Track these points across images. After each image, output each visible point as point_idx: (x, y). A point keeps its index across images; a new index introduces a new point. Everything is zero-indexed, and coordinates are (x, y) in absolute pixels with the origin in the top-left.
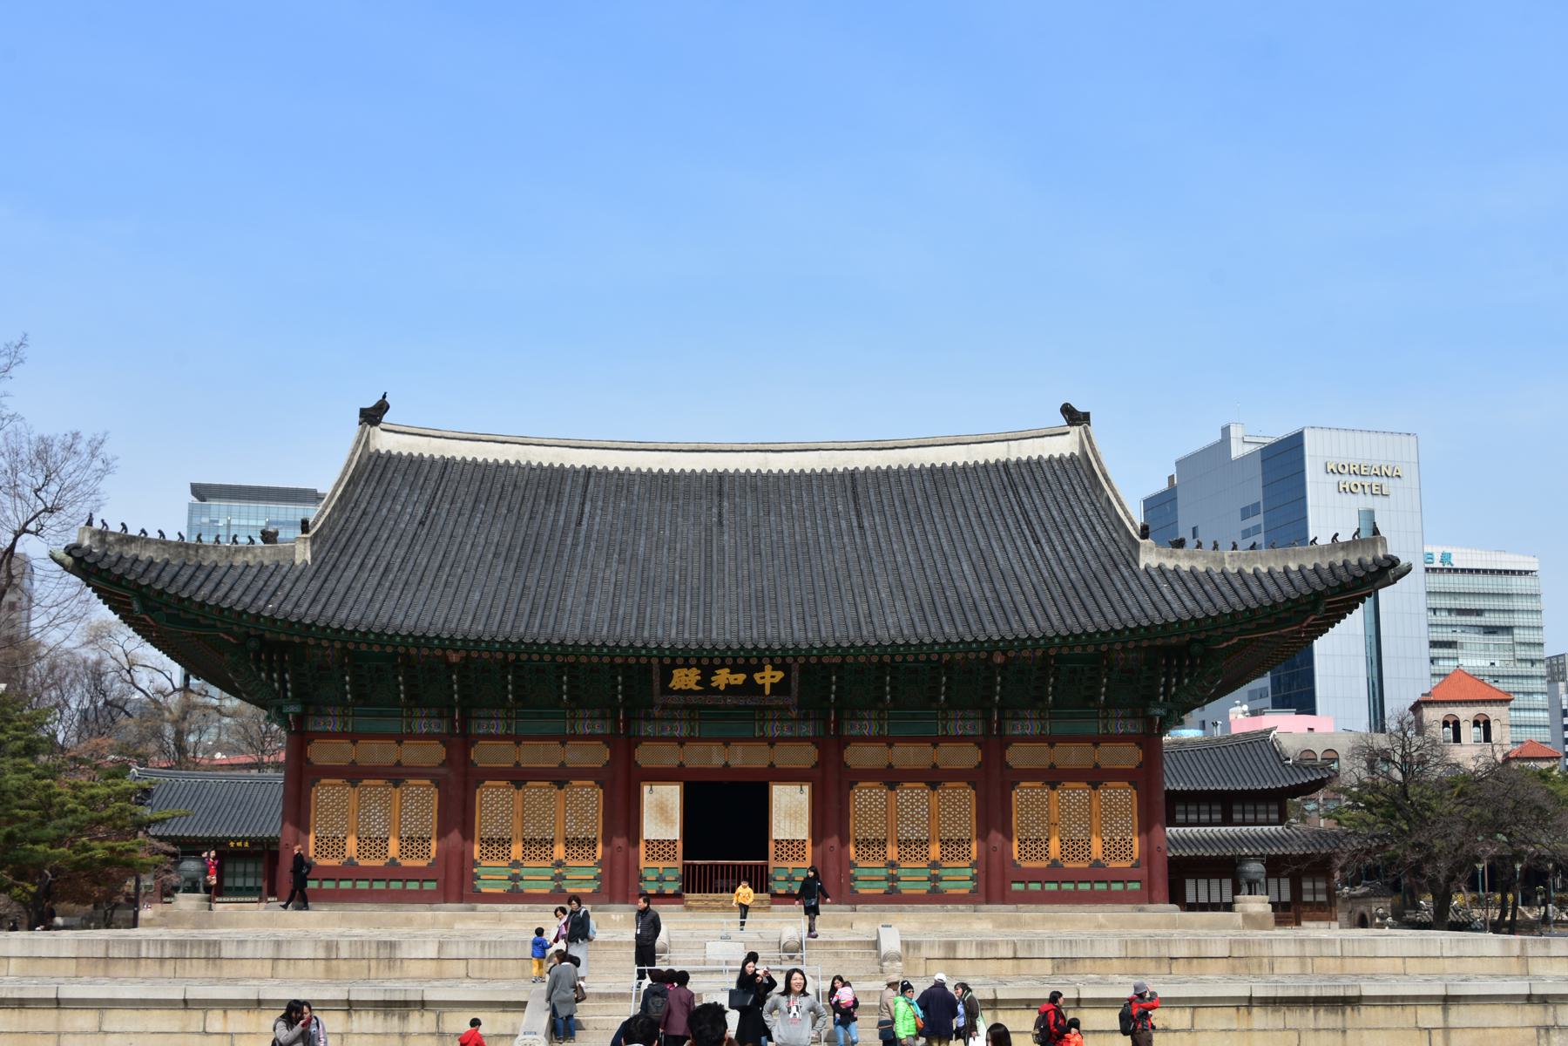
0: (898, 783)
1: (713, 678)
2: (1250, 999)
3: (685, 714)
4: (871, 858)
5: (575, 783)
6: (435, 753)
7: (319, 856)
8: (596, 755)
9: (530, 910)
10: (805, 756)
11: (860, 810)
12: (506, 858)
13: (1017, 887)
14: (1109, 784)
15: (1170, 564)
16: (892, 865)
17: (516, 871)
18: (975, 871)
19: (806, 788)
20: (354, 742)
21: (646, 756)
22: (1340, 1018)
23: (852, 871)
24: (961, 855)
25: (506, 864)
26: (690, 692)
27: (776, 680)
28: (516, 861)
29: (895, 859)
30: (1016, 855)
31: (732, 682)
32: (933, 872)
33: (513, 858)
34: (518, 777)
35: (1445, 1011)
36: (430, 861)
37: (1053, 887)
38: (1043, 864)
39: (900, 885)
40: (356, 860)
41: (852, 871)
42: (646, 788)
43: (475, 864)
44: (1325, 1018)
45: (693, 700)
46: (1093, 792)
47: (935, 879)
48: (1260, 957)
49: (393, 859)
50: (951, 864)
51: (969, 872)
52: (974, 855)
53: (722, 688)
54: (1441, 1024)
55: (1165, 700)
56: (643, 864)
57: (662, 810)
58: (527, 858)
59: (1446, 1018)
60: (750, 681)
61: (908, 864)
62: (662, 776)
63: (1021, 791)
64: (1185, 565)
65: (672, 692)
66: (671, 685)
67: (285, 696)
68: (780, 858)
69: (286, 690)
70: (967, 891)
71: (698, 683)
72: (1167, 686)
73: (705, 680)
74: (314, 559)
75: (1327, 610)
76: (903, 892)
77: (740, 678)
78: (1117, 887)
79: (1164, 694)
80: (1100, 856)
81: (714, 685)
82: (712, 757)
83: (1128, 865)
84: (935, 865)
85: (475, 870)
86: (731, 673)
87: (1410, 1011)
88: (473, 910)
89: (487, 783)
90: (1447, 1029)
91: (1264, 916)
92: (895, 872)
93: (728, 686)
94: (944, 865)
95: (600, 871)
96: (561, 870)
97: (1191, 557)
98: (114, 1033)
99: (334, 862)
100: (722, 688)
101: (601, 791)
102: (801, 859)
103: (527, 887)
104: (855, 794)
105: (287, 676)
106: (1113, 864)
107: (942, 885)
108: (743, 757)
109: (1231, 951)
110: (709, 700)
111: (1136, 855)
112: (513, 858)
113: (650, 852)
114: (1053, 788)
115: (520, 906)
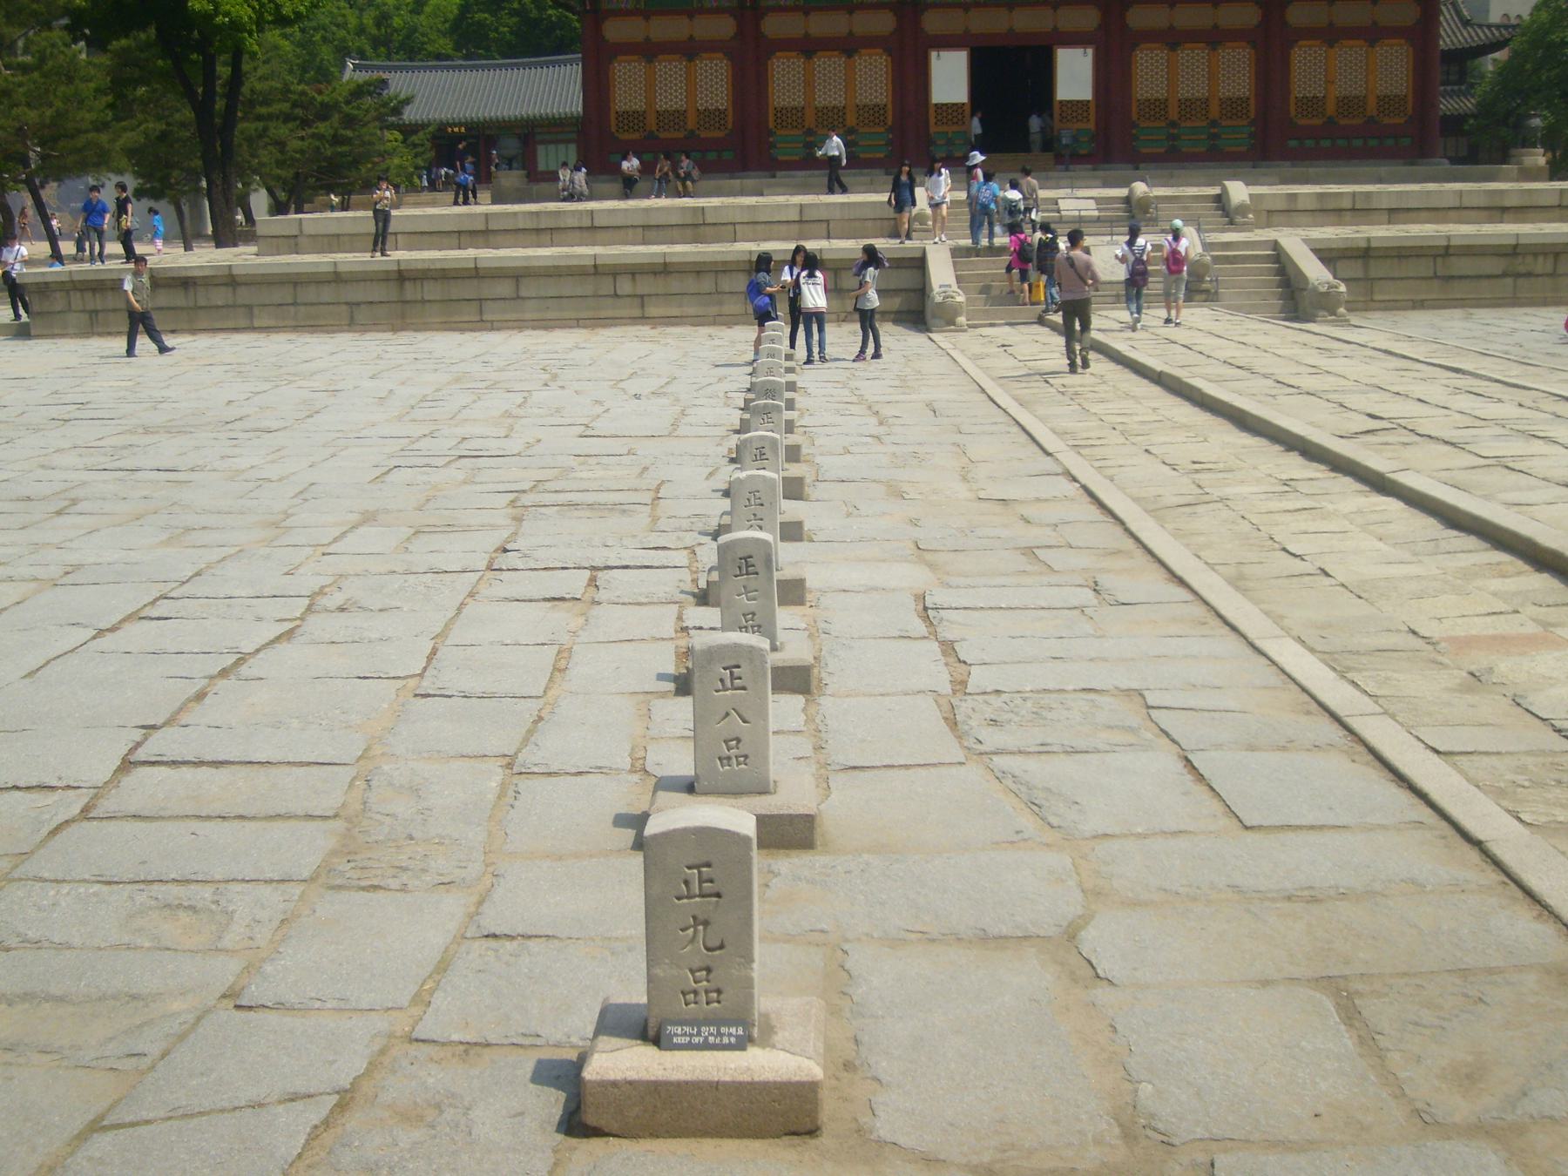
4: (1152, 118)
5: (863, 51)
6: (724, 27)
7: (621, 130)
8: (882, 23)
10: (1087, 18)
11: (1162, 70)
12: (799, 126)
13: (1293, 143)
14: (1386, 41)
16: (1173, 124)
18: (1253, 129)
19: (1090, 51)
20: (647, 18)
21: (933, 22)
23: (1134, 131)
24: (1240, 114)
25: (800, 132)
28: (809, 129)
29: (1176, 118)
30: (1293, 113)
32: (1212, 130)
33: (806, 127)
34: (808, 47)
36: (727, 132)
37: (1326, 143)
38: (1317, 122)
40: (656, 133)
41: (1134, 131)
42: (934, 54)
43: (770, 133)
46: (1370, 49)
47: (1215, 137)
49: (692, 132)
50: (1229, 122)
52: (1252, 115)
56: (933, 129)
58: (779, 127)
61: (1188, 124)
62: (948, 42)
63: (1300, 50)
68: (1065, 120)
70: (1244, 149)
76: (1184, 150)
78: (1390, 142)
80: (1375, 113)
82: (992, 23)
83: (1402, 121)
84: (1214, 123)
85: (771, 139)
88: (774, 176)
89: (778, 54)
91: (1540, 169)
92: (1176, 131)
94: (1224, 123)
95: (891, 136)
96: (853, 137)
98: (529, 298)
99: (636, 136)
101: (889, 59)
102: (1085, 120)
104: (1136, 56)
106: (1386, 121)
108: (1027, 21)
109: (1561, 199)
111: (1410, 111)
112: (806, 127)
113: (939, 117)
114: (1331, 46)
115: (816, 172)
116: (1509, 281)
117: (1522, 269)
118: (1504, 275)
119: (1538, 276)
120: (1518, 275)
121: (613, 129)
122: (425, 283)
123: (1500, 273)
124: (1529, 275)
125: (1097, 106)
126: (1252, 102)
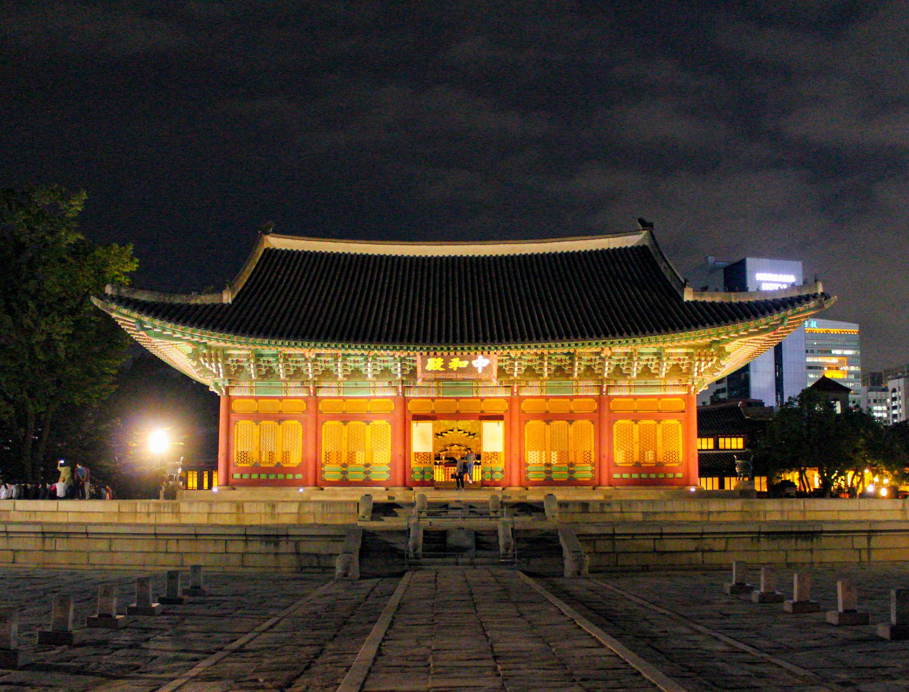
0: (551, 421)
1: (450, 364)
2: (759, 533)
3: (435, 384)
9: (352, 490)
15: (700, 299)
17: (345, 469)
22: (809, 543)
26: (438, 371)
27: (485, 365)
31: (461, 366)
35: (869, 539)
39: (554, 475)
44: (803, 544)
45: (440, 376)
48: (759, 512)
51: (590, 468)
53: (455, 369)
54: (866, 546)
55: (698, 375)
57: (423, 436)
59: (869, 543)
60: (470, 365)
64: (708, 299)
65: (427, 371)
66: (427, 368)
67: (219, 376)
69: (219, 373)
71: (442, 366)
72: (699, 368)
73: (445, 366)
74: (233, 301)
75: (790, 324)
77: (465, 364)
79: (698, 372)
81: (450, 367)
86: (461, 360)
87: (850, 538)
90: (869, 550)
93: (458, 368)
97: (712, 296)
100: (455, 369)
103: (351, 477)
105: (220, 365)
107: (576, 476)
110: (448, 376)
111: (681, 459)
115: (347, 488)
116: (699, 554)
117: (707, 548)
118: (696, 551)
119: (717, 551)
120: (704, 551)
121: (235, 461)
122: (58, 540)
123: (693, 549)
124: (711, 551)
125: (505, 454)
126: (593, 453)
